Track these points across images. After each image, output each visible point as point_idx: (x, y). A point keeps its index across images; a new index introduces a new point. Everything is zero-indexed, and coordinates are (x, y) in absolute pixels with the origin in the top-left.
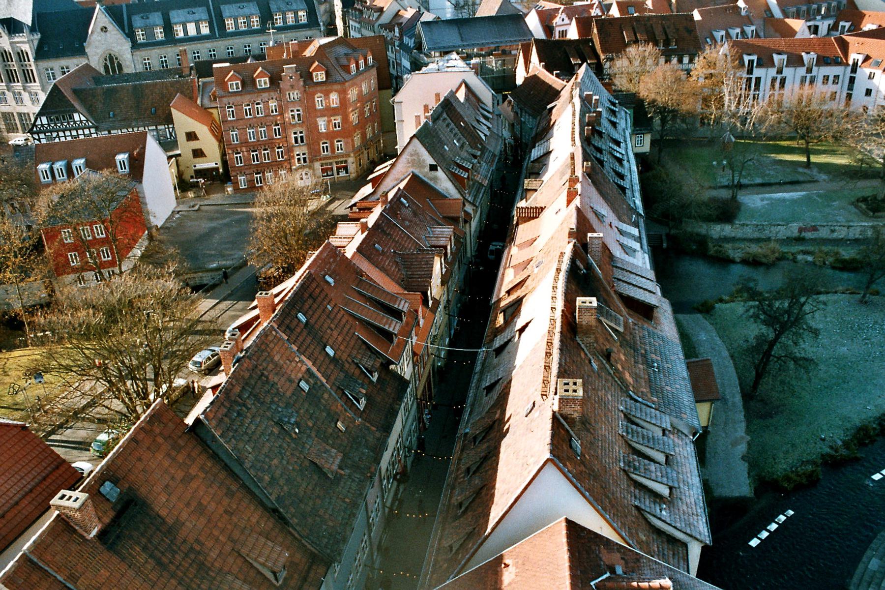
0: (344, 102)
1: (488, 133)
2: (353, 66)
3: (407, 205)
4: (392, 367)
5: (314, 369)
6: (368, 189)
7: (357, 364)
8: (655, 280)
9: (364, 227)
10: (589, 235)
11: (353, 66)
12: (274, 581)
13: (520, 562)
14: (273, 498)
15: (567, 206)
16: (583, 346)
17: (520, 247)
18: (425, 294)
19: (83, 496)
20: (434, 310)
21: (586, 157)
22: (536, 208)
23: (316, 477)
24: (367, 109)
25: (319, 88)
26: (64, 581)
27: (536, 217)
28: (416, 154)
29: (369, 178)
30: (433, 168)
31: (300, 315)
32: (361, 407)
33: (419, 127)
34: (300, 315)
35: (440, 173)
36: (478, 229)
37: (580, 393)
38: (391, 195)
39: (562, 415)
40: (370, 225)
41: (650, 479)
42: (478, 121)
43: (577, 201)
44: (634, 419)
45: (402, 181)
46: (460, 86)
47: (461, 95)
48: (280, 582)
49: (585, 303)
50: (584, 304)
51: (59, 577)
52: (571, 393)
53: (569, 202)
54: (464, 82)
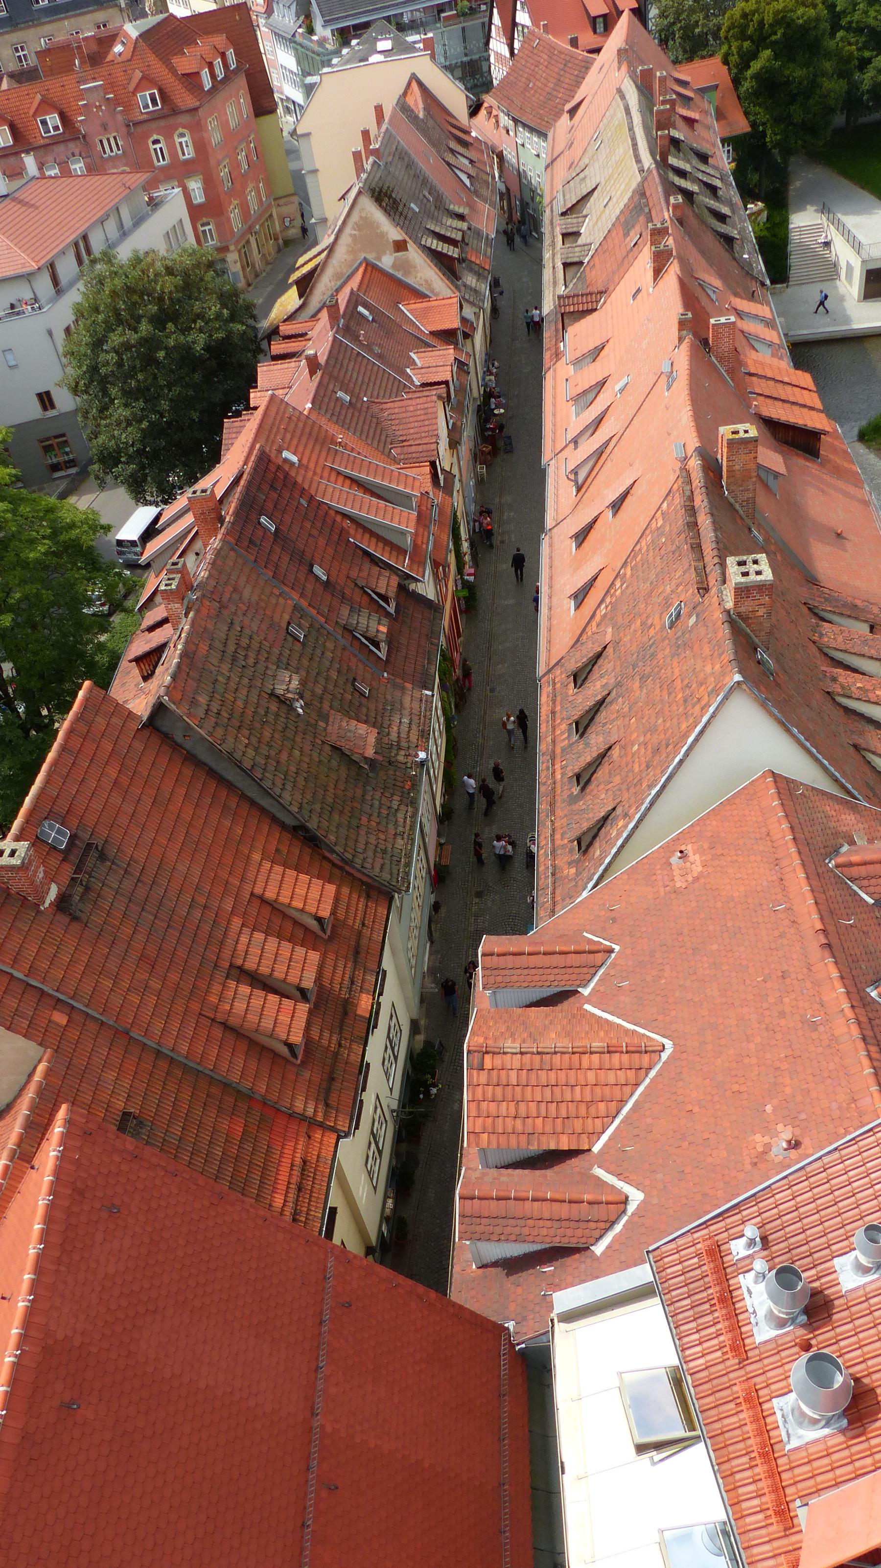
0: (201, 146)
1: (473, 172)
2: (205, 74)
3: (370, 318)
4: (412, 586)
5: (304, 603)
6: (290, 300)
7: (362, 588)
8: (812, 386)
9: (313, 364)
10: (712, 321)
11: (205, 74)
12: (321, 933)
13: (706, 845)
14: (294, 809)
15: (655, 280)
16: (737, 506)
17: (577, 362)
18: (433, 464)
19: (23, 847)
20: (448, 489)
21: (670, 189)
22: (591, 294)
23: (343, 773)
24: (242, 157)
25: (153, 125)
26: (25, 978)
27: (596, 310)
28: (367, 224)
29: (290, 281)
30: (400, 246)
31: (263, 520)
32: (383, 655)
33: (364, 176)
34: (263, 520)
35: (414, 254)
36: (484, 349)
37: (768, 575)
38: (343, 299)
39: (739, 615)
40: (322, 360)
41: (868, 701)
42: (452, 151)
43: (673, 270)
44: (822, 614)
45: (349, 278)
46: (409, 84)
47: (416, 101)
48: (329, 932)
49: (735, 432)
50: (737, 436)
51: (16, 974)
52: (753, 577)
53: (658, 272)
54: (414, 77)
